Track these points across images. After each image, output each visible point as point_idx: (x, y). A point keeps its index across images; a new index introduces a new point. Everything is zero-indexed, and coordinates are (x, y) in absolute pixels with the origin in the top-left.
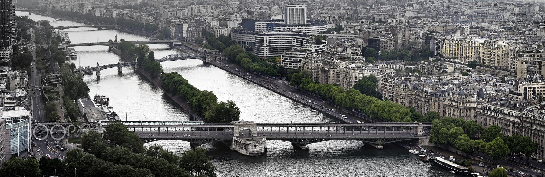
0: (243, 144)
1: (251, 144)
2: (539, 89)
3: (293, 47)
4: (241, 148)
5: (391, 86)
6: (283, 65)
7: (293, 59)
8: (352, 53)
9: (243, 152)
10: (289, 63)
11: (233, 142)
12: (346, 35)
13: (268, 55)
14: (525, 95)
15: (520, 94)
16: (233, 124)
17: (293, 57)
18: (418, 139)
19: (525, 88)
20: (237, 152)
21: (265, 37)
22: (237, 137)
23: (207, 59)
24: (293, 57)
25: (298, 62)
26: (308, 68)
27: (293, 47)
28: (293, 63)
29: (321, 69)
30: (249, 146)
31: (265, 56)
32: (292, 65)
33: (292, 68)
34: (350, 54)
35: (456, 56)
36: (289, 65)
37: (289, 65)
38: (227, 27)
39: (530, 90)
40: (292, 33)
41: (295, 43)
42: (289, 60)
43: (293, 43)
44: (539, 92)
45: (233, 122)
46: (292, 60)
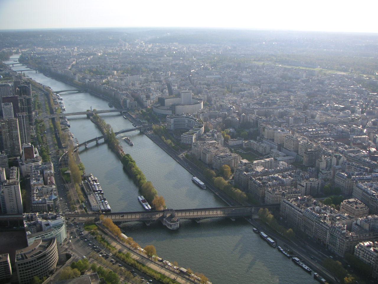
1: (173, 224)
2: (314, 184)
3: (186, 124)
4: (169, 226)
8: (217, 137)
9: (169, 228)
14: (306, 187)
15: (303, 186)
19: (306, 184)
20: (166, 226)
21: (172, 119)
23: (142, 130)
25: (190, 140)
27: (186, 124)
30: (172, 226)
31: (172, 129)
33: (187, 143)
39: (309, 184)
44: (313, 186)
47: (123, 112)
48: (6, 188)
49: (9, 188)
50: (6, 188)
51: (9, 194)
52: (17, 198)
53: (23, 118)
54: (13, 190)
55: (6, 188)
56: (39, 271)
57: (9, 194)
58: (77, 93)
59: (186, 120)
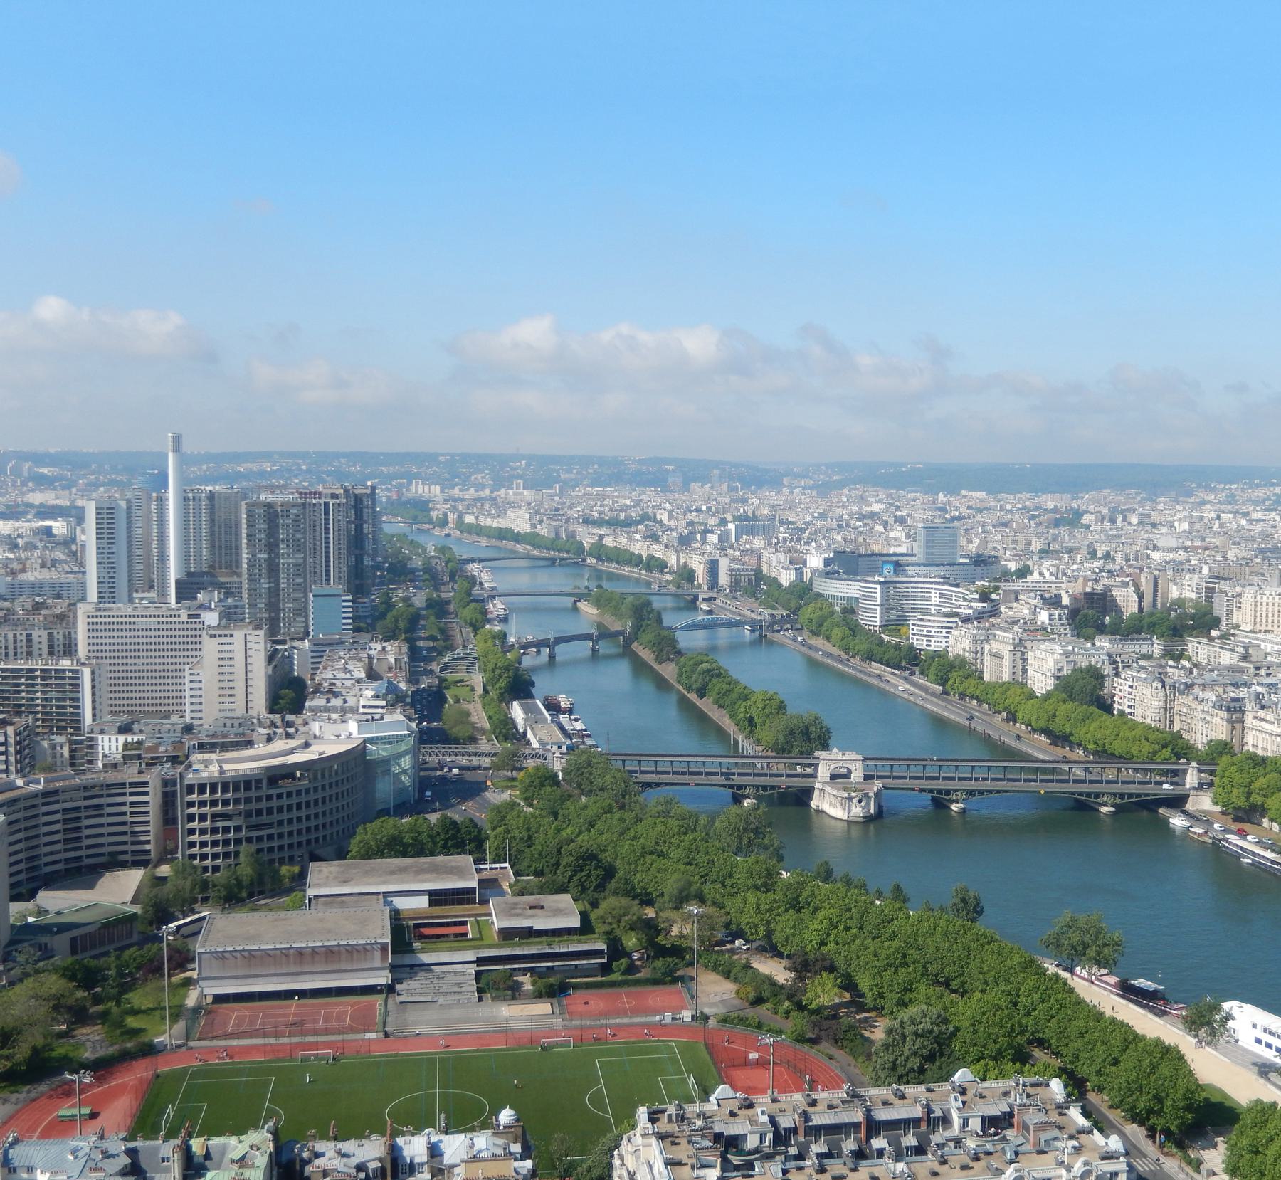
0: (836, 797)
3: (933, 608)
4: (832, 805)
5: (1131, 687)
6: (915, 642)
7: (933, 630)
8: (1050, 620)
10: (925, 639)
11: (816, 793)
12: (1038, 585)
13: (884, 623)
16: (818, 758)
17: (933, 627)
18: (1188, 796)
20: (822, 812)
22: (824, 783)
24: (933, 627)
26: (964, 650)
28: (933, 639)
29: (989, 651)
31: (878, 624)
32: (932, 643)
34: (1047, 622)
35: (1269, 628)
36: (925, 643)
37: (925, 643)
38: (805, 565)
40: (932, 580)
41: (938, 599)
42: (925, 633)
43: (933, 599)
45: (817, 754)
46: (933, 633)
47: (704, 600)
48: (215, 636)
49: (223, 640)
50: (211, 636)
51: (222, 663)
52: (250, 682)
53: (327, 513)
54: (238, 647)
55: (215, 636)
56: (270, 837)
57: (222, 663)
58: (548, 566)
59: (933, 595)
